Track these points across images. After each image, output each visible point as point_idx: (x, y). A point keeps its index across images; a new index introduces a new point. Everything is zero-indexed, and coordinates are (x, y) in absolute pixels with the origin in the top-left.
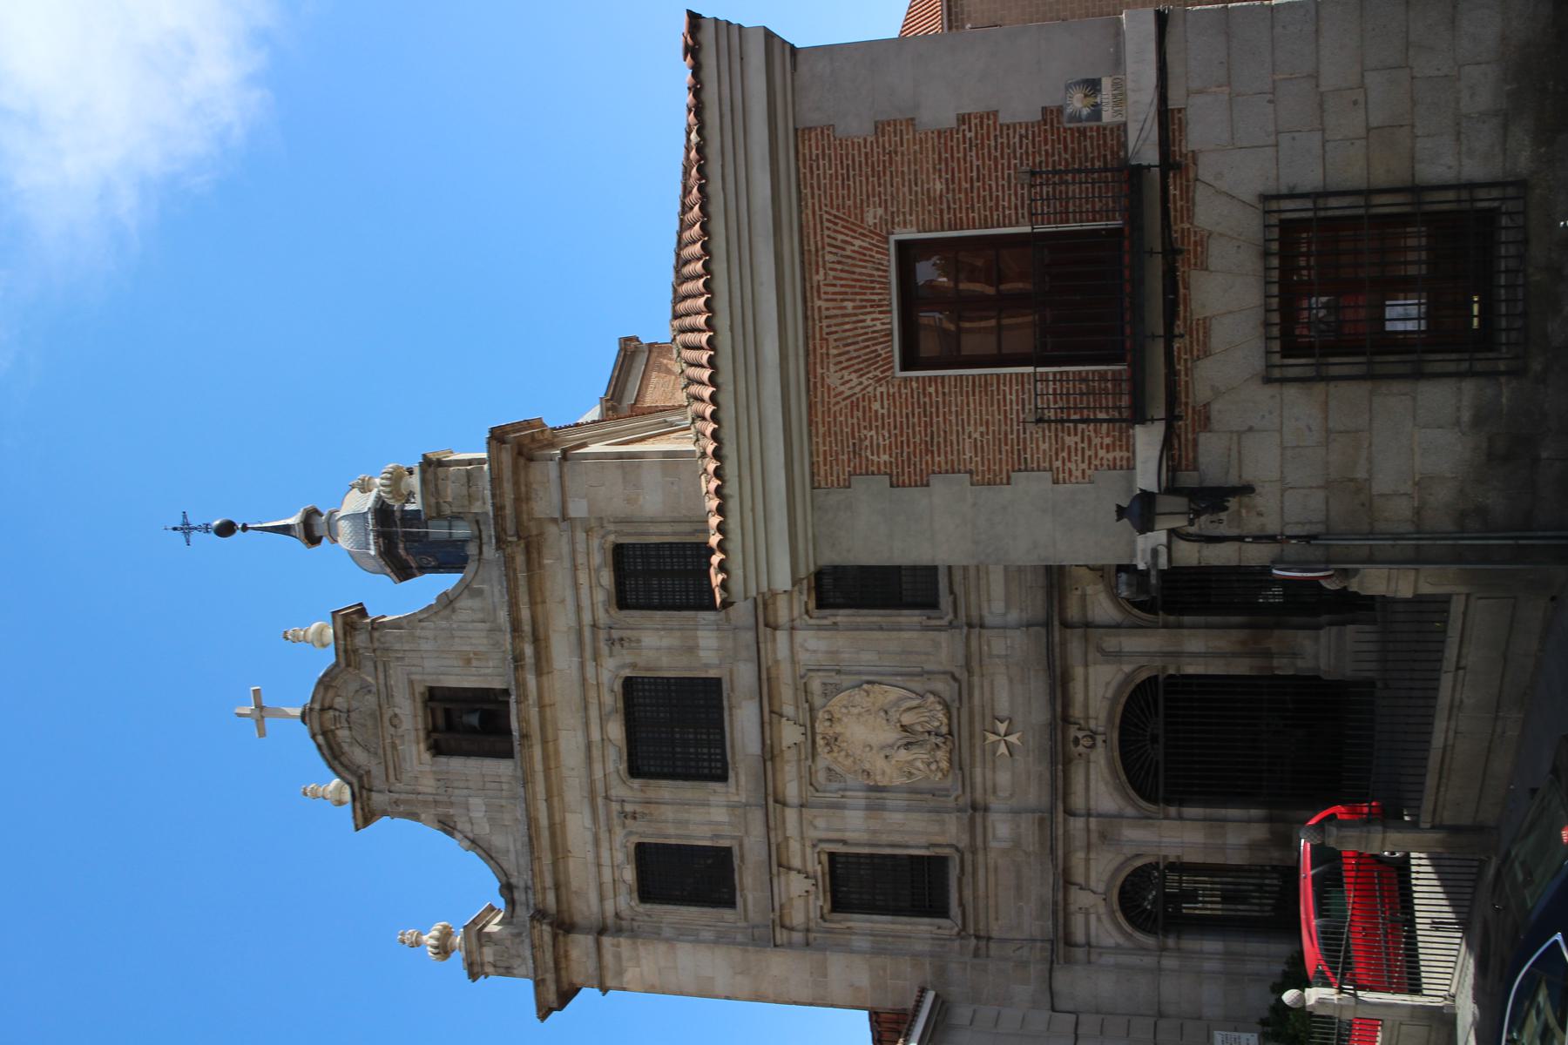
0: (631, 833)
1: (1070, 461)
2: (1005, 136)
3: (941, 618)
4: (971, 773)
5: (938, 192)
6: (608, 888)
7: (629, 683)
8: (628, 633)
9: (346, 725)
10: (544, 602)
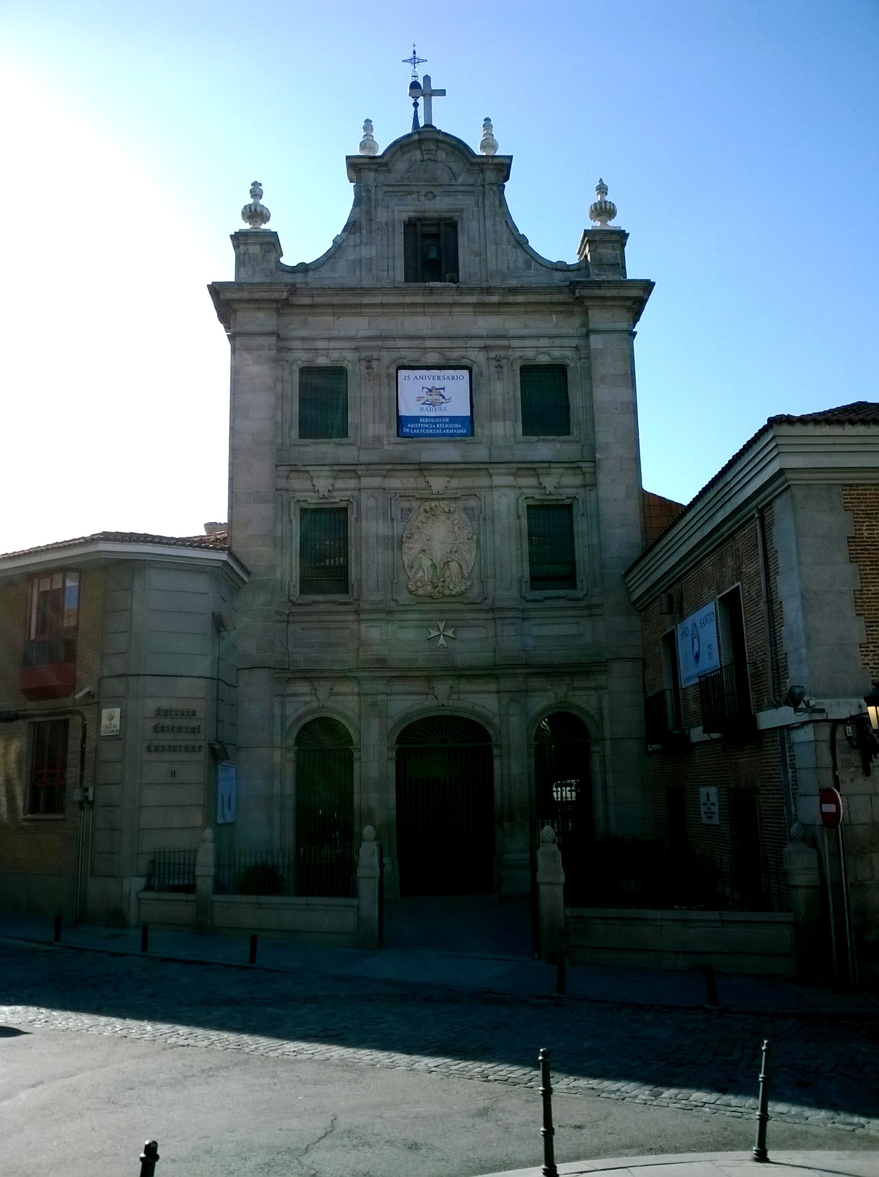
1: (874, 655)
4: (413, 611)
6: (311, 345)
8: (506, 370)
9: (425, 157)
10: (526, 313)
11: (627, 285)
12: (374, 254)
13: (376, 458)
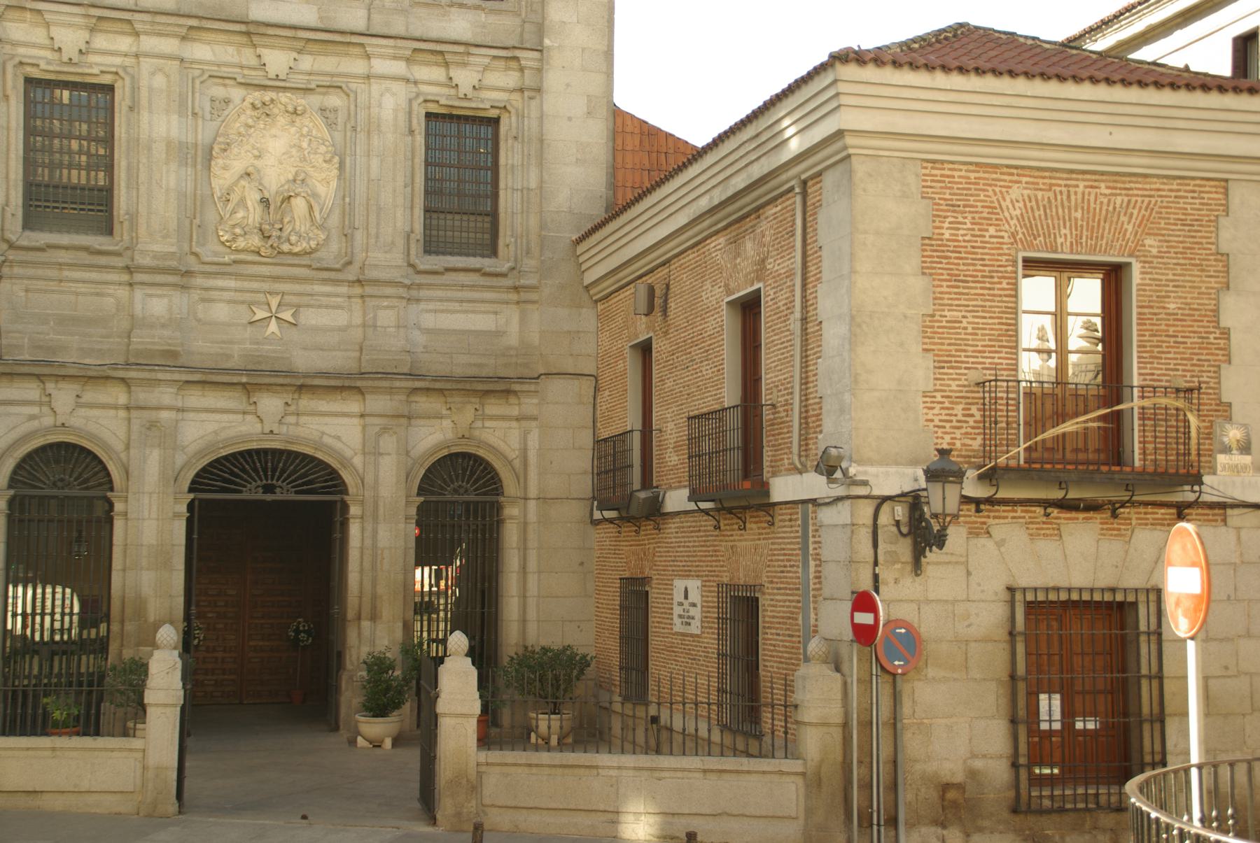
2: (1209, 369)
4: (230, 274)
5: (1167, 306)
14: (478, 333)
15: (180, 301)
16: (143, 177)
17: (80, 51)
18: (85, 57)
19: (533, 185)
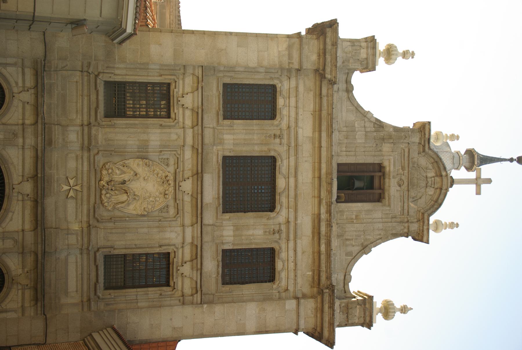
0: (277, 126)
3: (103, 252)
4: (90, 168)
6: (293, 94)
7: (272, 209)
9: (429, 180)
10: (313, 253)
11: (331, 328)
12: (359, 141)
13: (207, 141)
14: (66, 283)
15: (76, 146)
16: (132, 130)
17: (183, 105)
18: (181, 107)
19: (139, 304)
